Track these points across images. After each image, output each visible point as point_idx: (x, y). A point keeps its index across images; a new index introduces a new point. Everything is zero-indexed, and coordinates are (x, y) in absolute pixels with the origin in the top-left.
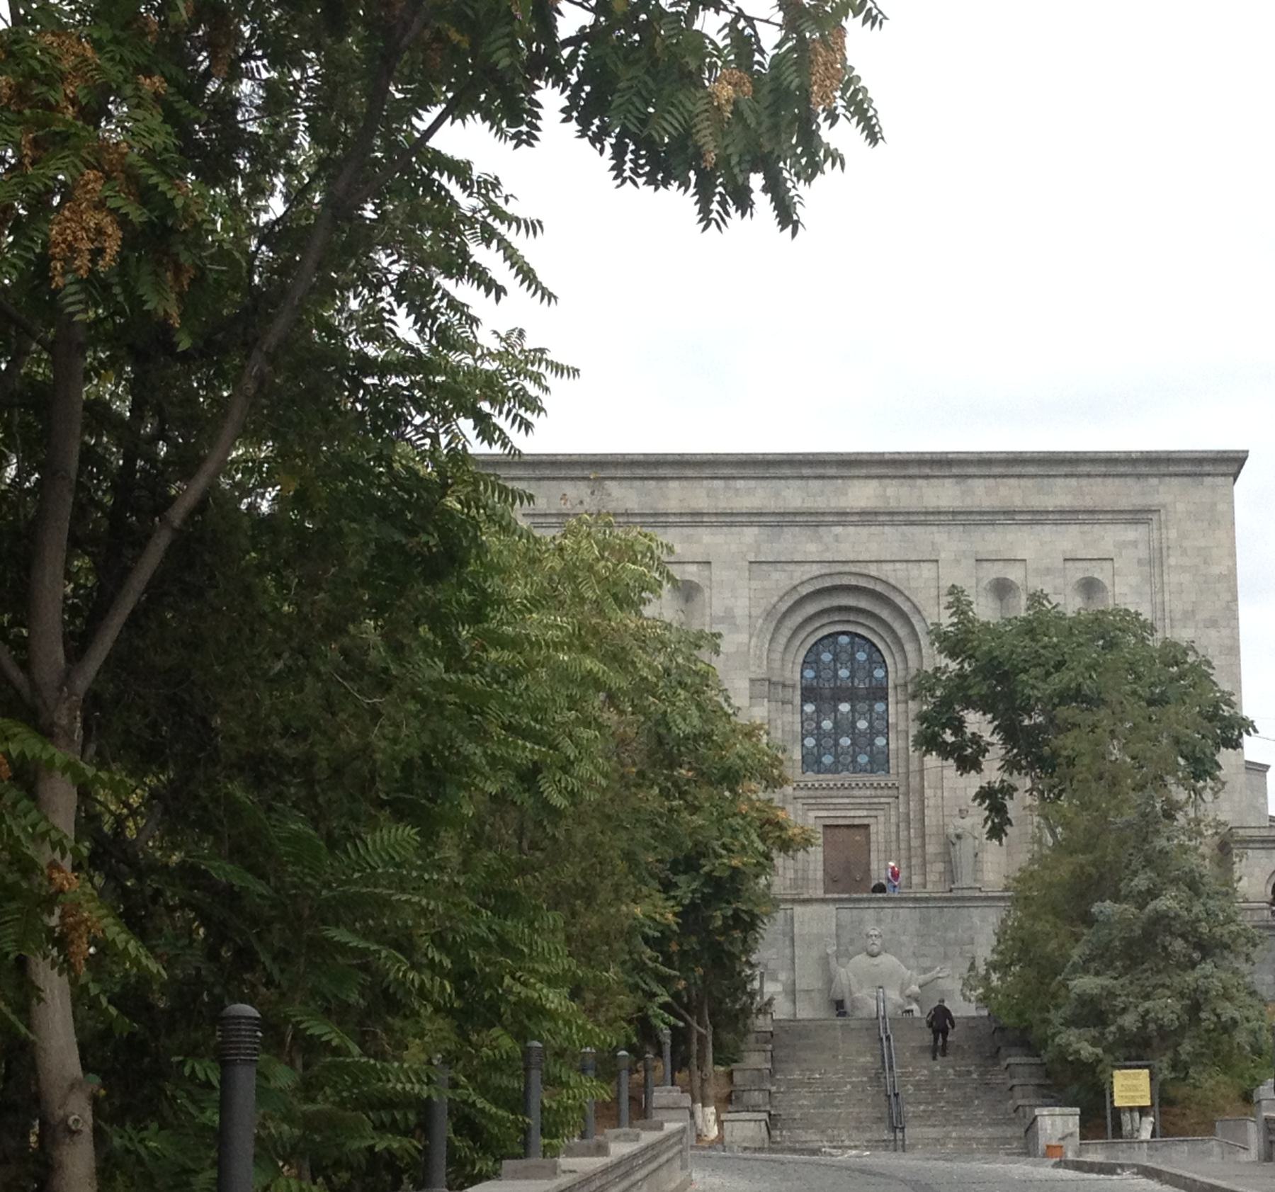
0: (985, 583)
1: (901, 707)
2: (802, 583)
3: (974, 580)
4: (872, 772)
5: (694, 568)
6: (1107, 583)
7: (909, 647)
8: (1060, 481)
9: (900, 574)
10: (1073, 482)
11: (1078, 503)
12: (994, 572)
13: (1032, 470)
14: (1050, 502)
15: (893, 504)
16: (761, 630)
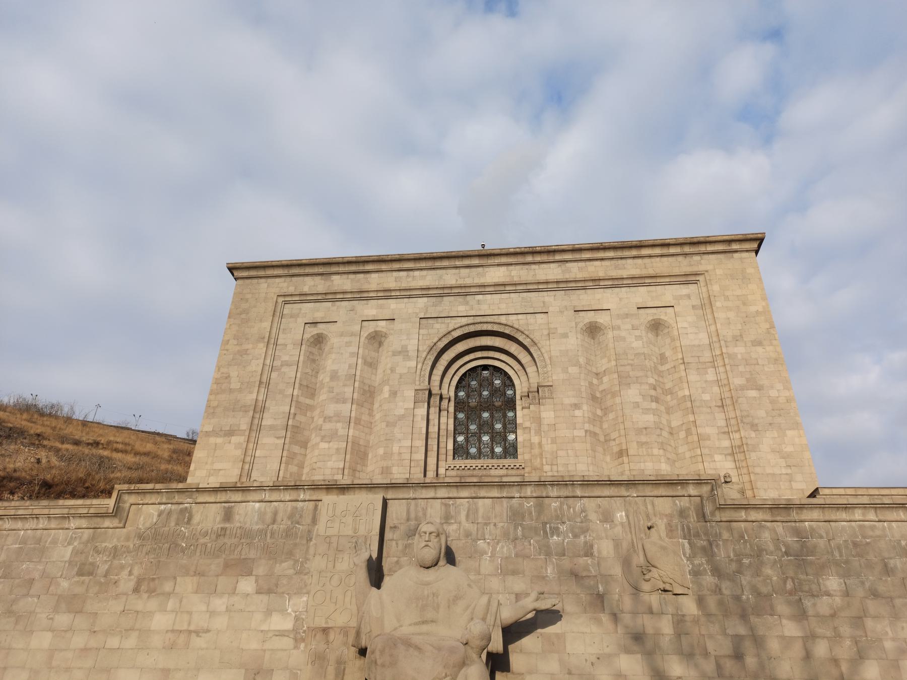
0: (581, 325)
1: (526, 411)
2: (455, 329)
3: (574, 323)
4: (505, 458)
5: (383, 323)
6: (672, 322)
7: (531, 370)
8: (630, 261)
9: (521, 322)
10: (639, 261)
11: (644, 272)
12: (589, 317)
13: (611, 254)
14: (625, 274)
15: (516, 280)
16: (425, 359)
